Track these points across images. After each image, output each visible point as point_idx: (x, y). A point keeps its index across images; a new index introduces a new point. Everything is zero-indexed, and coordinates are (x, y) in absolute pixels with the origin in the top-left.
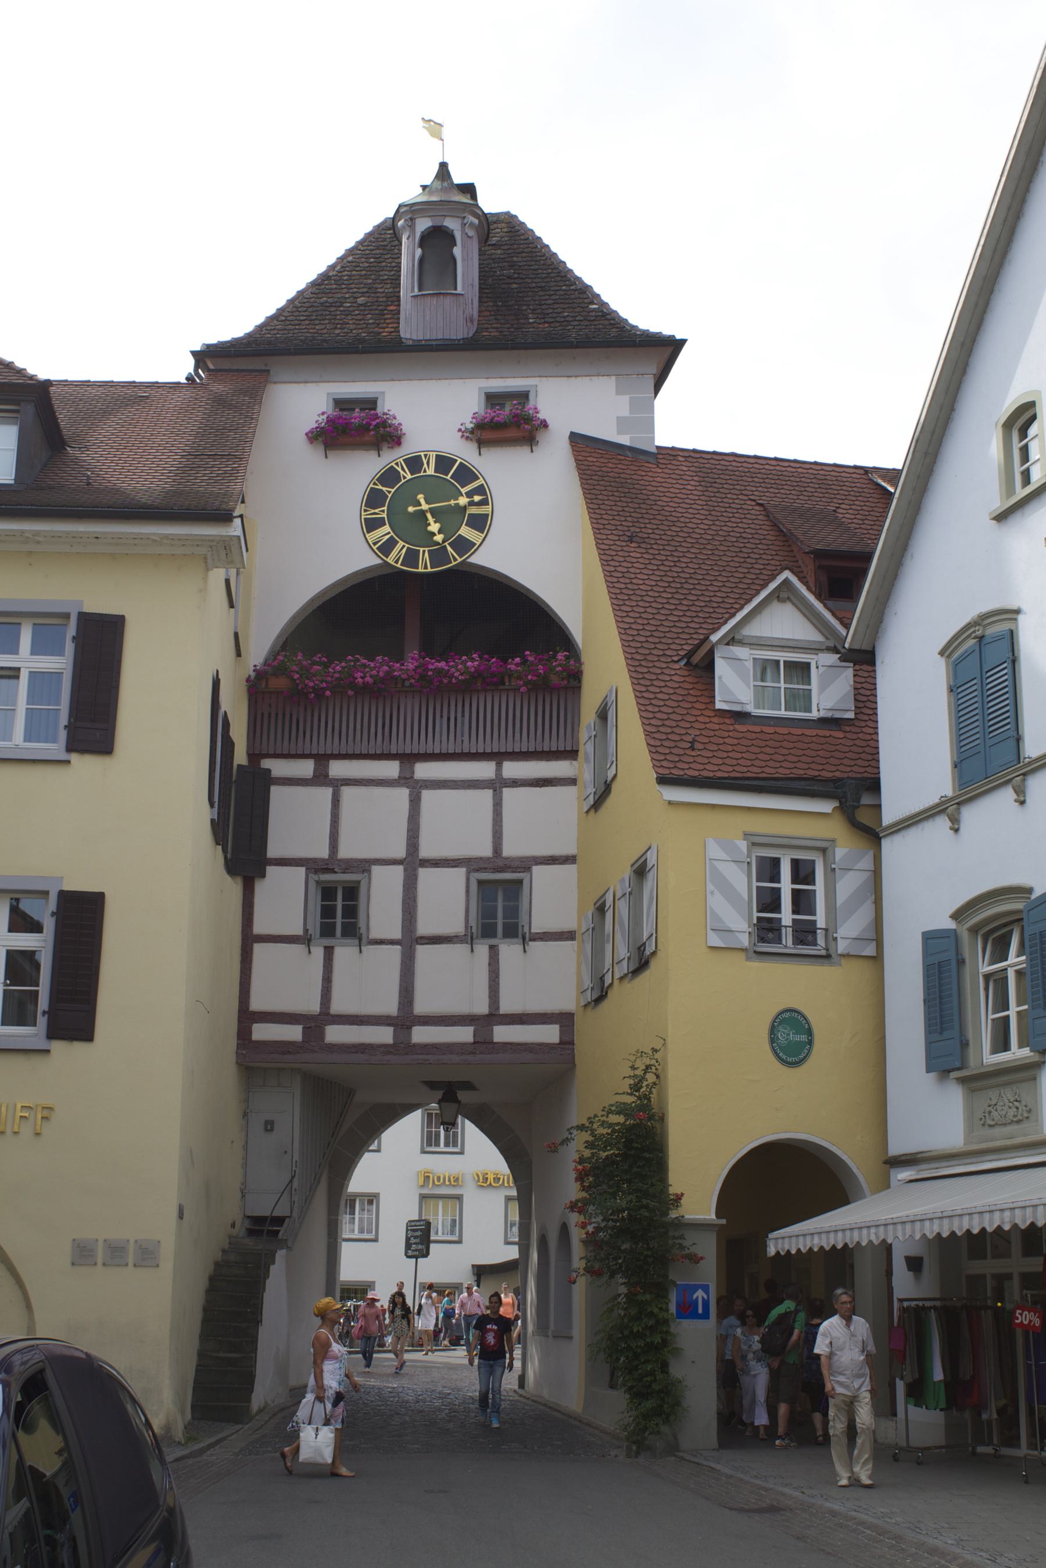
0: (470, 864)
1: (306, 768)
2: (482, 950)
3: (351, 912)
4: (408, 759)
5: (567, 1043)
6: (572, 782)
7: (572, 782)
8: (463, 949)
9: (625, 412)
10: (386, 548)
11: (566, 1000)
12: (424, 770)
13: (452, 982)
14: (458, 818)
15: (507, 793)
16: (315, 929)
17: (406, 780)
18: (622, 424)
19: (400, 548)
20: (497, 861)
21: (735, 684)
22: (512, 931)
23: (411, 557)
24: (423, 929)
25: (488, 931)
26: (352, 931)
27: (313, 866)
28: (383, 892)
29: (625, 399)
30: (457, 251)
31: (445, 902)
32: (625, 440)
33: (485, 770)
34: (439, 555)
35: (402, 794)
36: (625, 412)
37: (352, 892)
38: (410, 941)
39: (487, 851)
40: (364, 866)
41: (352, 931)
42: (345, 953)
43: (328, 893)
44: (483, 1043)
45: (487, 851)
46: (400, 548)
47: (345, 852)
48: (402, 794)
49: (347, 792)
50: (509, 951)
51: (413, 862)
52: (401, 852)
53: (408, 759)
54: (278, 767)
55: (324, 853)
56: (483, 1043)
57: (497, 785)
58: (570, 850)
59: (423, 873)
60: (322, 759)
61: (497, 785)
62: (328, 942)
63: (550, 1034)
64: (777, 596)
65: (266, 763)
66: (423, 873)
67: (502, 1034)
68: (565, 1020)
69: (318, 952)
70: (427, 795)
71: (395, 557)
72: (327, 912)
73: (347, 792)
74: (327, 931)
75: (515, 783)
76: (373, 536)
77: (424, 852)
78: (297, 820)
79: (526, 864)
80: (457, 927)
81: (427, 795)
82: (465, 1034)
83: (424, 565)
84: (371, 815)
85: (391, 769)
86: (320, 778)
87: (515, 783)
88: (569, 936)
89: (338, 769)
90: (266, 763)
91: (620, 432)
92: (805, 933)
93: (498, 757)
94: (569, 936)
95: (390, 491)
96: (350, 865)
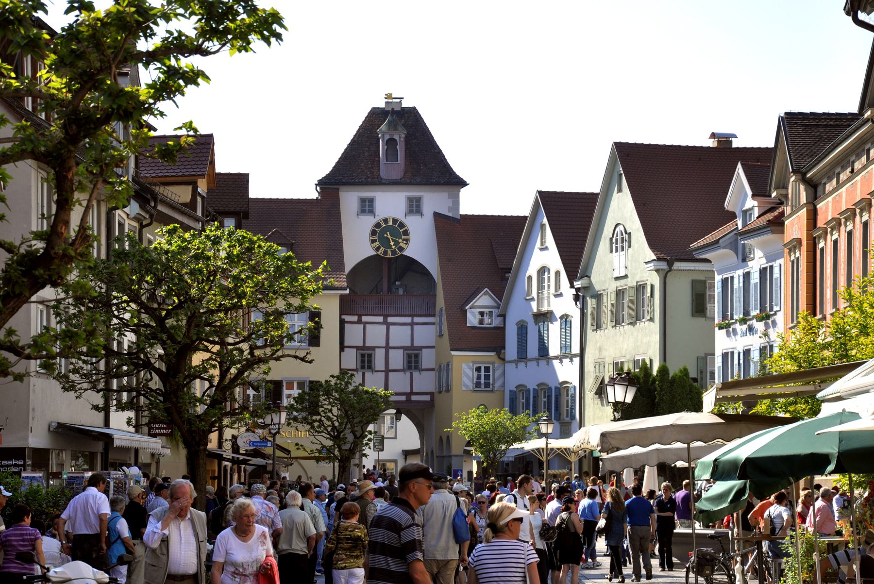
0: (405, 348)
1: (355, 318)
2: (408, 374)
3: (370, 361)
4: (386, 316)
5: (432, 400)
6: (434, 324)
7: (434, 324)
8: (402, 373)
9: (451, 205)
10: (378, 249)
11: (431, 388)
12: (390, 320)
13: (399, 383)
14: (400, 335)
15: (415, 327)
16: (359, 367)
17: (385, 322)
18: (450, 209)
19: (382, 249)
20: (412, 347)
21: (473, 319)
22: (417, 368)
23: (385, 253)
24: (391, 368)
25: (410, 368)
26: (370, 367)
27: (358, 348)
28: (379, 355)
29: (451, 200)
30: (398, 147)
31: (397, 359)
32: (450, 214)
33: (408, 320)
34: (394, 252)
35: (384, 327)
36: (451, 205)
37: (370, 356)
38: (387, 371)
39: (409, 344)
40: (373, 348)
41: (370, 367)
42: (368, 375)
43: (363, 356)
44: (409, 400)
45: (409, 344)
46: (382, 249)
47: (367, 345)
48: (384, 327)
49: (368, 326)
50: (416, 374)
51: (387, 348)
52: (384, 345)
53: (386, 316)
54: (347, 318)
55: (361, 344)
56: (409, 400)
57: (412, 324)
58: (434, 344)
59: (391, 351)
60: (360, 316)
61: (412, 324)
62: (363, 371)
63: (427, 398)
64: (485, 294)
65: (343, 317)
66: (391, 351)
67: (414, 398)
68: (431, 394)
69: (361, 374)
70: (391, 327)
71: (381, 252)
72: (363, 361)
73: (368, 326)
74: (363, 367)
75: (417, 324)
76: (373, 245)
77: (391, 345)
78: (354, 335)
79: (421, 348)
80: (400, 367)
81: (391, 327)
82: (403, 398)
83: (389, 255)
84: (376, 335)
85: (380, 319)
86: (359, 322)
87: (417, 324)
88: (433, 370)
89: (365, 319)
90: (343, 317)
91: (449, 211)
92: (487, 385)
93: (412, 316)
94: (433, 370)
95: (378, 230)
96: (369, 348)
